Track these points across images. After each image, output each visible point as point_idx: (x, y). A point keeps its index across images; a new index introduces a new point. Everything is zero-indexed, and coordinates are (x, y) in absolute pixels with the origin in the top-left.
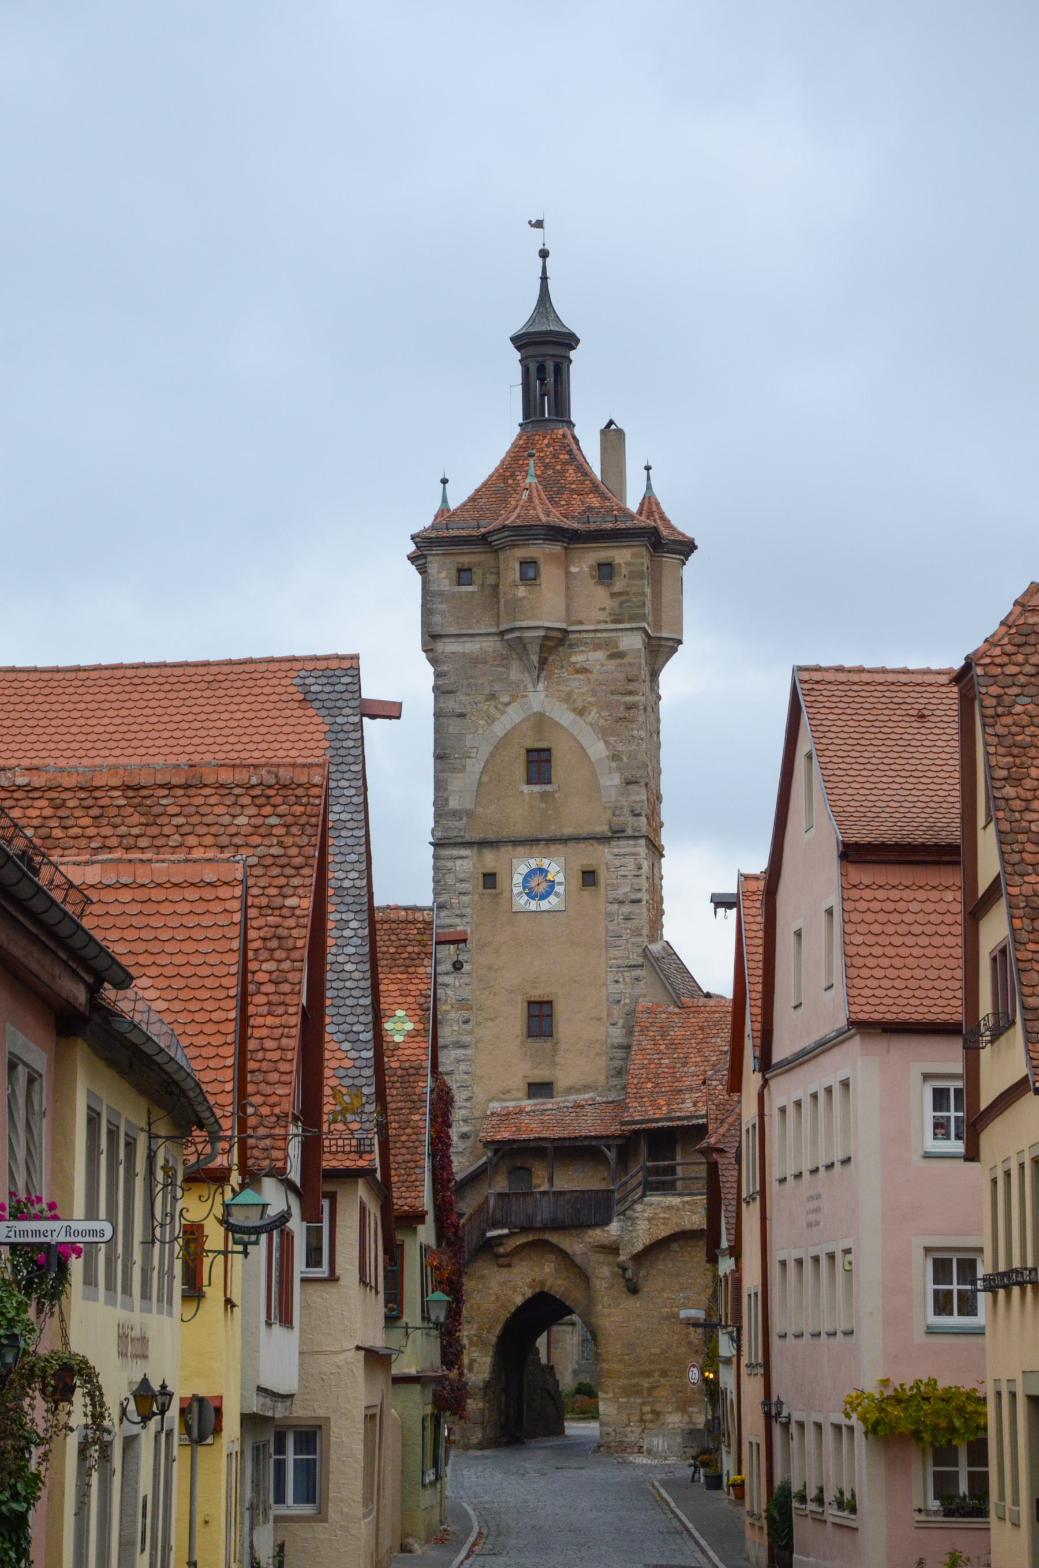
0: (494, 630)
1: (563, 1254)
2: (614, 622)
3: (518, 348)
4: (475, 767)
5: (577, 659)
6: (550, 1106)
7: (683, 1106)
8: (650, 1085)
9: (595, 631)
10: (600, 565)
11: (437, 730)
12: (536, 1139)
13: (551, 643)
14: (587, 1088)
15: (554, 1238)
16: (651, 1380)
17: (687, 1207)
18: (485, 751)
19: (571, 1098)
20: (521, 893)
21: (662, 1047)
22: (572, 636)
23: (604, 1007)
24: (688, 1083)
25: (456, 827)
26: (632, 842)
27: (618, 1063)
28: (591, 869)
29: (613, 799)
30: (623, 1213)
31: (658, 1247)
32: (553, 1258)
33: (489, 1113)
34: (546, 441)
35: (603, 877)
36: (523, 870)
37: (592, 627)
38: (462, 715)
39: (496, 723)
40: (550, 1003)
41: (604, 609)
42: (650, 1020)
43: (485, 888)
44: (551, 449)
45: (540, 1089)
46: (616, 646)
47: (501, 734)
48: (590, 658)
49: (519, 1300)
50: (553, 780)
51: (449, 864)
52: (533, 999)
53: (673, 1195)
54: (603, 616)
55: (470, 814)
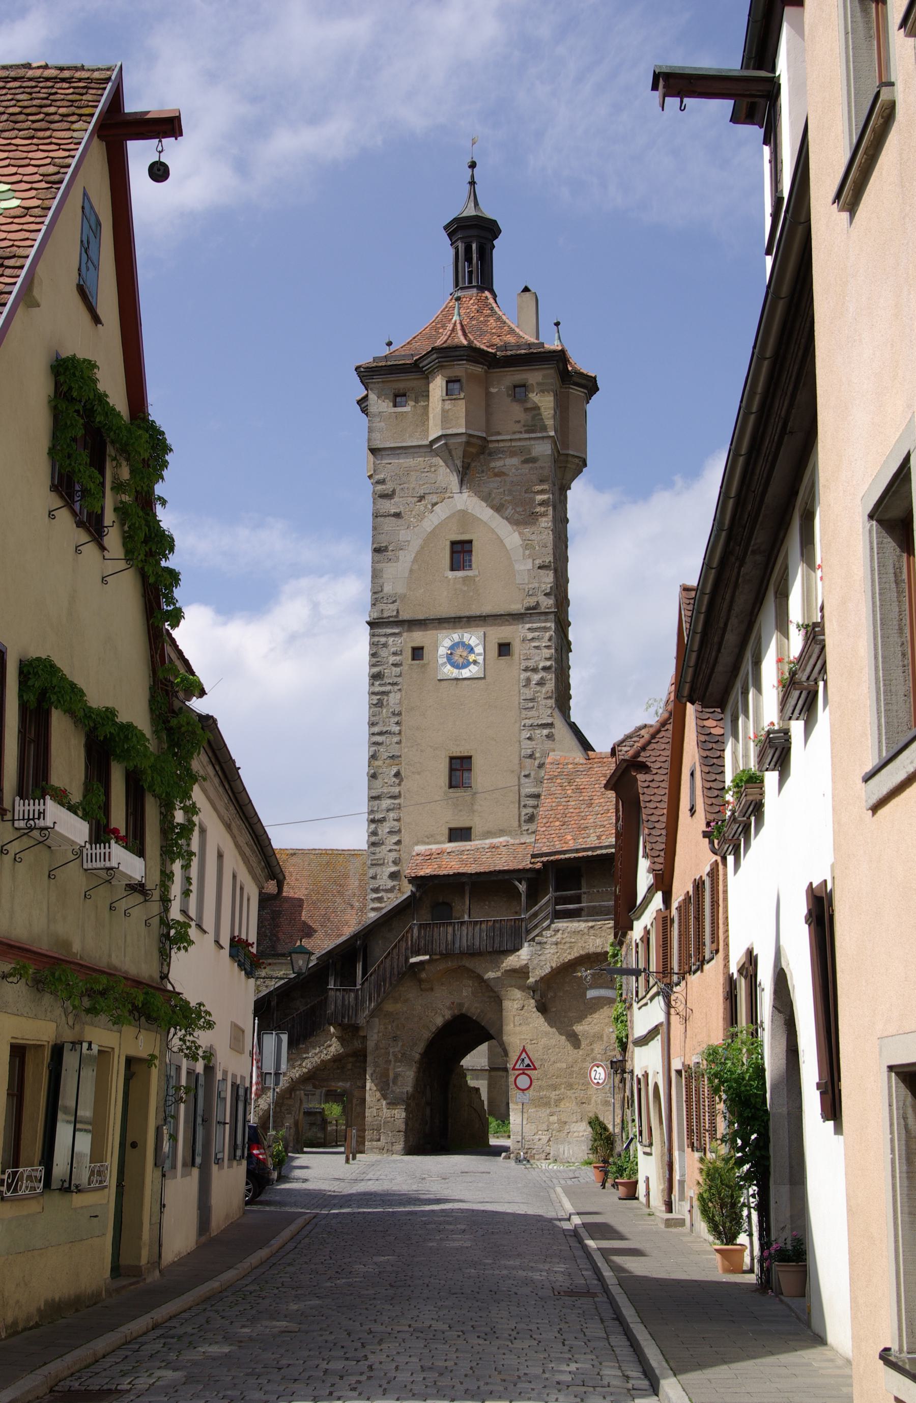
0: (426, 442)
1: (480, 979)
2: (527, 432)
3: (450, 235)
4: (406, 558)
5: (497, 464)
6: (468, 848)
7: (589, 840)
8: (557, 823)
9: (511, 440)
10: (515, 387)
11: (375, 528)
12: (454, 874)
13: (472, 450)
14: (502, 832)
15: (468, 963)
16: (557, 1093)
17: (592, 931)
18: (416, 545)
19: (487, 841)
20: (445, 663)
21: (569, 792)
22: (491, 446)
23: (516, 761)
24: (591, 821)
25: (389, 611)
26: (543, 618)
27: (529, 810)
28: (507, 641)
29: (526, 581)
30: (533, 940)
31: (566, 970)
32: (470, 983)
33: (414, 854)
34: (472, 302)
35: (518, 648)
36: (448, 643)
37: (509, 437)
38: (397, 515)
39: (426, 520)
40: (470, 758)
41: (519, 422)
42: (559, 770)
43: (413, 659)
44: (476, 307)
45: (459, 834)
46: (529, 452)
47: (429, 530)
48: (507, 463)
49: (439, 1021)
50: (474, 566)
51: (383, 640)
52: (454, 755)
53: (579, 921)
54: (517, 427)
55: (403, 597)
